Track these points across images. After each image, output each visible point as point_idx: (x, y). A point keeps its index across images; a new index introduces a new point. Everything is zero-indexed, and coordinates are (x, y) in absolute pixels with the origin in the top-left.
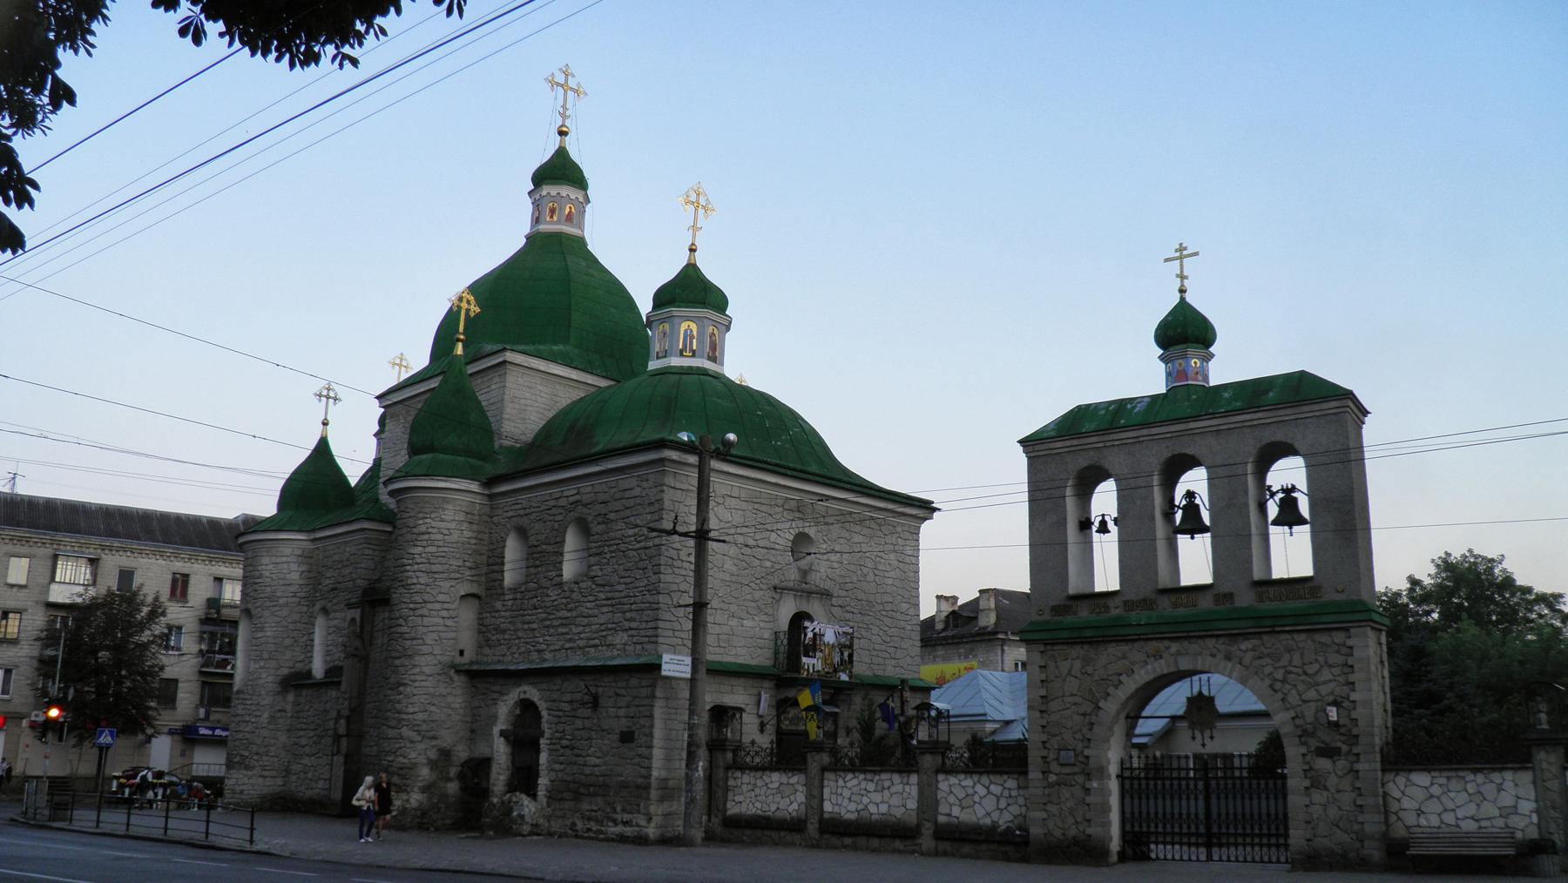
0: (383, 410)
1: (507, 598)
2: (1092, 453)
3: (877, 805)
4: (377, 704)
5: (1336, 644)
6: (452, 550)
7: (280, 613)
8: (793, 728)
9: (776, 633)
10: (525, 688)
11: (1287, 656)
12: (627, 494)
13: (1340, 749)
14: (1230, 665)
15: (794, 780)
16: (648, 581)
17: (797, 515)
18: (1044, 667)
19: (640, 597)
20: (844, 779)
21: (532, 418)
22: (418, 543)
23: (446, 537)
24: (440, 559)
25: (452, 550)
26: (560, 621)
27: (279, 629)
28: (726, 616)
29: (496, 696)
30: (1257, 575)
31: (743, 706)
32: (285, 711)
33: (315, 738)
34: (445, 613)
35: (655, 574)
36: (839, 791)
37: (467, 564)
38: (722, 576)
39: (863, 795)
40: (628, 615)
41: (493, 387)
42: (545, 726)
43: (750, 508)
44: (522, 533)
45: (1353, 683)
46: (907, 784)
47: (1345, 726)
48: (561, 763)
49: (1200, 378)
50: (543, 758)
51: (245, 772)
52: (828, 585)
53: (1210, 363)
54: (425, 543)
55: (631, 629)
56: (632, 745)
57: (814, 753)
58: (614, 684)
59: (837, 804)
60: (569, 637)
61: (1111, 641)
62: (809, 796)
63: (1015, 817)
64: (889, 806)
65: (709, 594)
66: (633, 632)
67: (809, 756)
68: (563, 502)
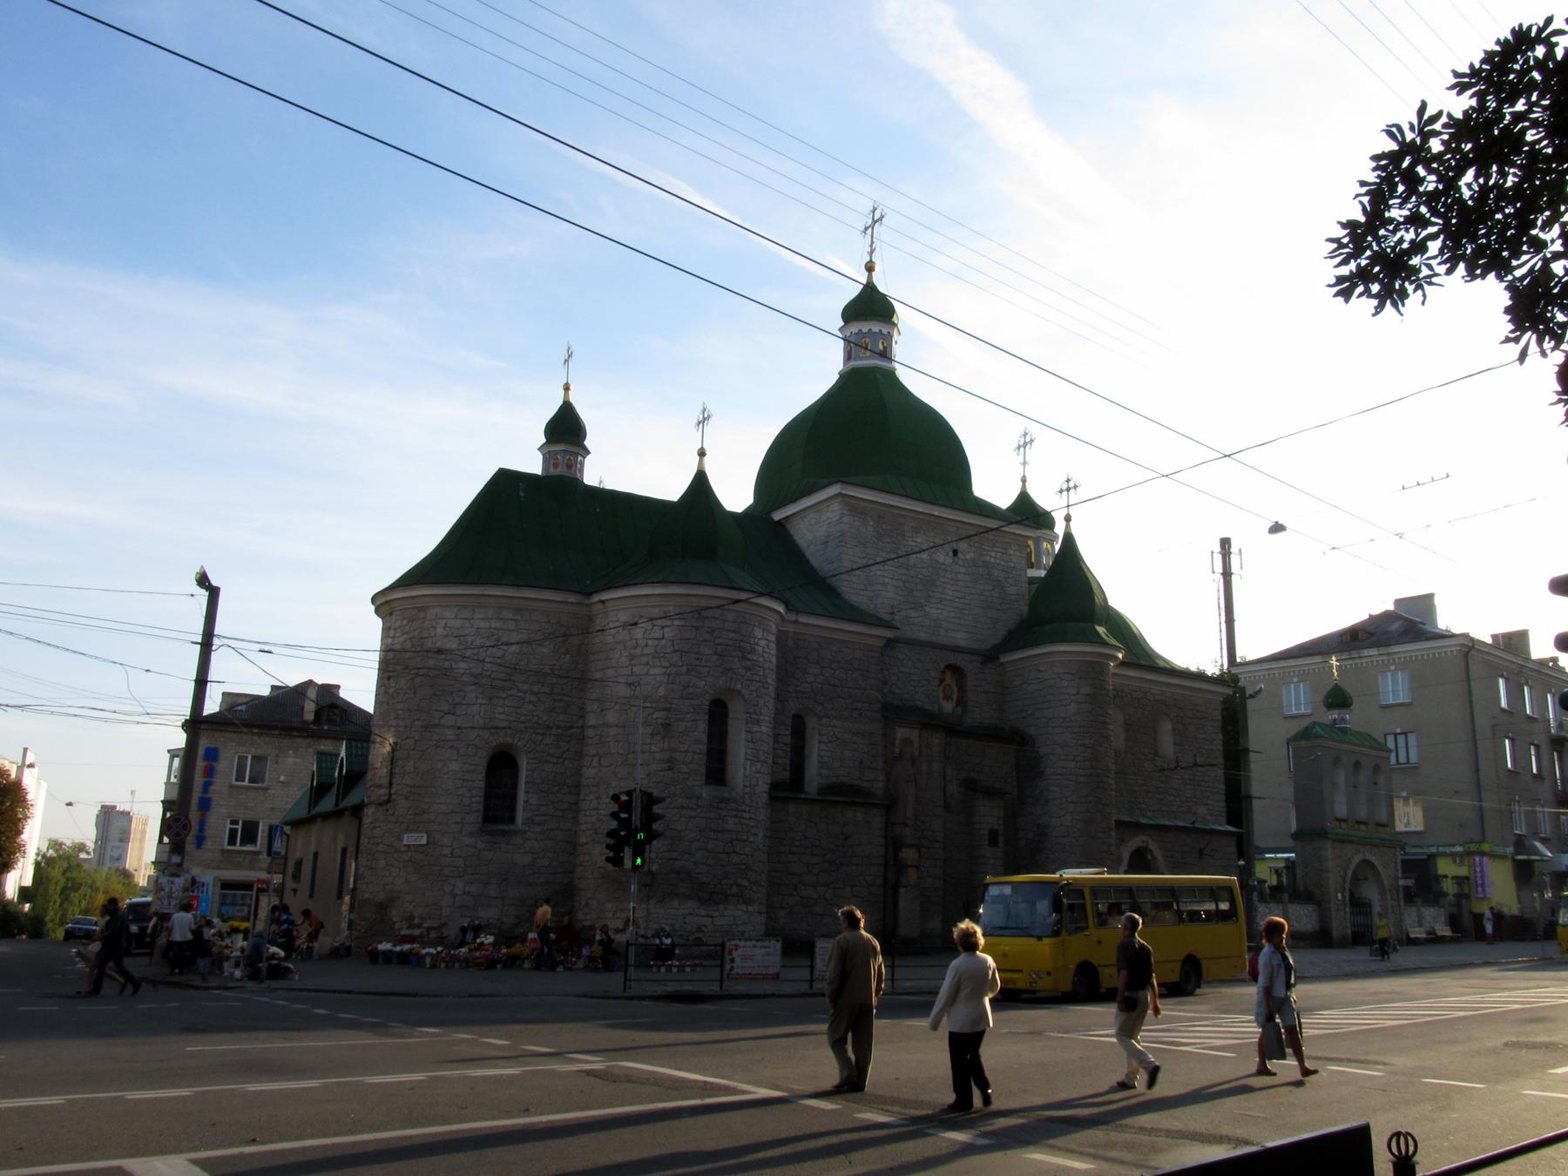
51: (744, 908)
55: (1208, 804)
68: (1152, 699)
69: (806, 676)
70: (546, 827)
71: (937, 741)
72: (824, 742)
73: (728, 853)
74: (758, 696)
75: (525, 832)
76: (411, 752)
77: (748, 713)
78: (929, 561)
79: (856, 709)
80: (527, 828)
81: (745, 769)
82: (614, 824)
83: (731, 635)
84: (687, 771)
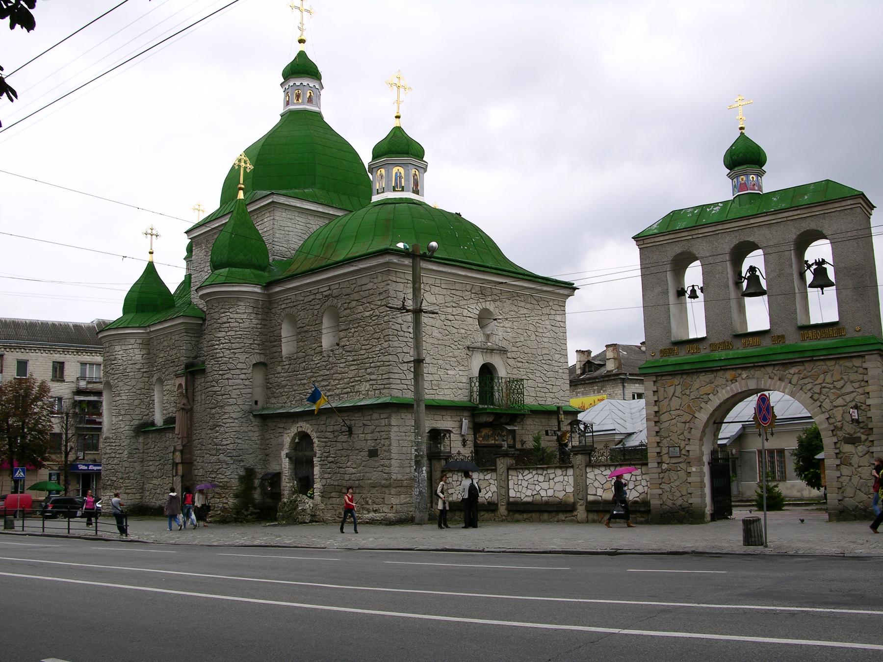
0: (190, 240)
1: (285, 363)
2: (684, 243)
3: (546, 490)
4: (200, 441)
5: (855, 367)
6: (245, 333)
7: (130, 383)
8: (486, 443)
9: (470, 378)
10: (300, 424)
11: (822, 376)
12: (364, 288)
13: (860, 437)
14: (783, 384)
15: (488, 477)
16: (381, 346)
17: (480, 296)
18: (657, 391)
19: (377, 358)
20: (522, 474)
21: (294, 240)
22: (223, 330)
23: (241, 325)
24: (238, 339)
25: (245, 333)
27: (132, 394)
28: (436, 368)
29: (281, 430)
30: (801, 322)
31: (451, 429)
32: (138, 449)
33: (160, 466)
34: (243, 376)
35: (385, 341)
36: (520, 482)
37: (256, 342)
38: (431, 341)
39: (536, 485)
40: (369, 371)
41: (266, 220)
42: (316, 449)
43: (449, 293)
44: (292, 319)
45: (868, 393)
46: (566, 475)
47: (863, 422)
48: (329, 473)
49: (756, 188)
50: (317, 470)
52: (504, 344)
53: (763, 177)
54: (226, 330)
55: (371, 380)
56: (376, 459)
57: (500, 458)
58: (362, 418)
59: (518, 492)
60: (329, 387)
61: (701, 372)
62: (499, 487)
63: (640, 494)
64: (554, 491)
65: (424, 354)
66: (373, 382)
67: (498, 460)
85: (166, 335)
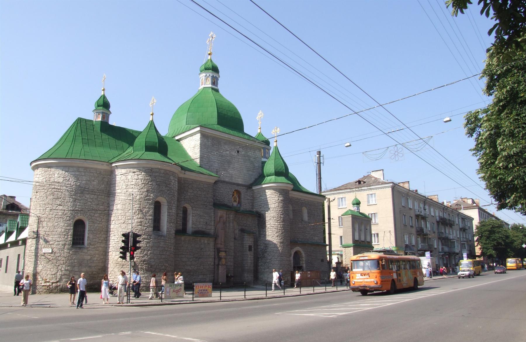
26: (302, 232)
55: (318, 236)
60: (305, 236)
66: (319, 237)
69: (188, 193)
70: (95, 246)
71: (232, 216)
72: (194, 216)
73: (161, 255)
74: (171, 200)
75: (88, 248)
76: (45, 219)
77: (168, 205)
78: (229, 155)
79: (205, 205)
80: (88, 247)
81: (167, 225)
82: (123, 245)
83: (162, 178)
84: (147, 226)
85: (196, 181)
